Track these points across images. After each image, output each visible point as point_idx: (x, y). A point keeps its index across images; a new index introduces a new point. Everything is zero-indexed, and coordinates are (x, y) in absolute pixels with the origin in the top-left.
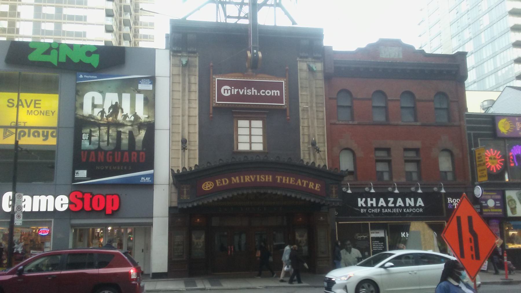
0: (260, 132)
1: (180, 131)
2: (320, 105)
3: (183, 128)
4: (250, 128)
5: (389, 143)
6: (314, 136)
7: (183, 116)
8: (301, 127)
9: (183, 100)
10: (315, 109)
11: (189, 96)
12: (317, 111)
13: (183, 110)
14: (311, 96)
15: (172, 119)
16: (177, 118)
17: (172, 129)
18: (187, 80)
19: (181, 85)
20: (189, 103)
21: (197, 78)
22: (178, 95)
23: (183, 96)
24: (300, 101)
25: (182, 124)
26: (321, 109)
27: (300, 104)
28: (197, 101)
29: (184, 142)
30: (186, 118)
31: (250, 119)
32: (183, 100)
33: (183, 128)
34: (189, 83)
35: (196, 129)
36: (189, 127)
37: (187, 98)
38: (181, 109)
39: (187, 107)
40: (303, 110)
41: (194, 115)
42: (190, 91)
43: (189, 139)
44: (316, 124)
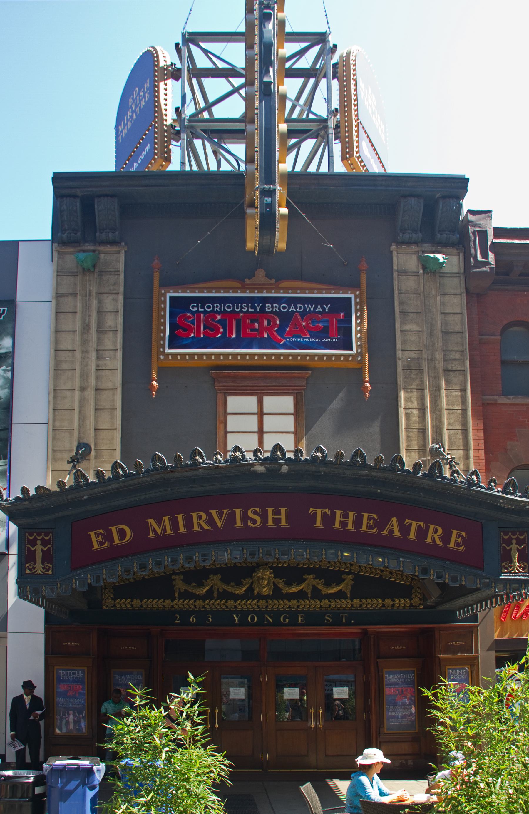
2: (457, 356)
4: (261, 414)
7: (83, 389)
9: (85, 352)
10: (440, 365)
11: (99, 341)
12: (446, 370)
13: (84, 376)
14: (431, 334)
15: (55, 397)
16: (68, 393)
17: (54, 421)
18: (94, 303)
19: (78, 315)
20: (98, 358)
21: (121, 298)
23: (84, 342)
24: (399, 346)
25: (81, 407)
26: (456, 366)
27: (399, 353)
28: (119, 354)
30: (90, 394)
31: (260, 392)
32: (85, 352)
36: (96, 418)
37: (93, 346)
39: (93, 367)
40: (407, 368)
41: (110, 385)
42: (100, 331)
43: (96, 444)
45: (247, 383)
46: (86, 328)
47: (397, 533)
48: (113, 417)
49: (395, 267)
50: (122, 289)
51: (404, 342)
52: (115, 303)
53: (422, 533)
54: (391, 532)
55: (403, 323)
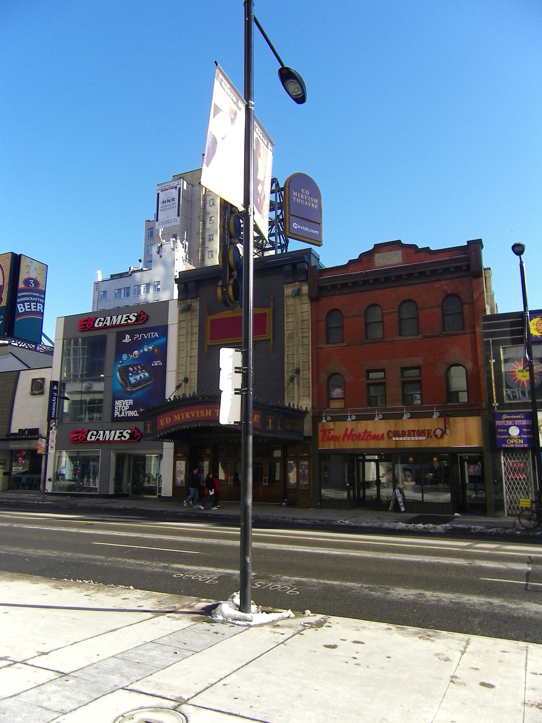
1: (184, 371)
3: (186, 368)
7: (187, 357)
8: (286, 356)
13: (187, 352)
20: (191, 344)
22: (183, 339)
23: (187, 339)
24: (285, 329)
26: (306, 335)
28: (197, 342)
29: (186, 380)
30: (189, 358)
33: (186, 368)
34: (192, 327)
35: (195, 368)
38: (184, 351)
40: (288, 338)
44: (300, 351)
46: (187, 333)
48: (195, 367)
50: (198, 317)
51: (287, 327)
52: (196, 323)
55: (287, 319)
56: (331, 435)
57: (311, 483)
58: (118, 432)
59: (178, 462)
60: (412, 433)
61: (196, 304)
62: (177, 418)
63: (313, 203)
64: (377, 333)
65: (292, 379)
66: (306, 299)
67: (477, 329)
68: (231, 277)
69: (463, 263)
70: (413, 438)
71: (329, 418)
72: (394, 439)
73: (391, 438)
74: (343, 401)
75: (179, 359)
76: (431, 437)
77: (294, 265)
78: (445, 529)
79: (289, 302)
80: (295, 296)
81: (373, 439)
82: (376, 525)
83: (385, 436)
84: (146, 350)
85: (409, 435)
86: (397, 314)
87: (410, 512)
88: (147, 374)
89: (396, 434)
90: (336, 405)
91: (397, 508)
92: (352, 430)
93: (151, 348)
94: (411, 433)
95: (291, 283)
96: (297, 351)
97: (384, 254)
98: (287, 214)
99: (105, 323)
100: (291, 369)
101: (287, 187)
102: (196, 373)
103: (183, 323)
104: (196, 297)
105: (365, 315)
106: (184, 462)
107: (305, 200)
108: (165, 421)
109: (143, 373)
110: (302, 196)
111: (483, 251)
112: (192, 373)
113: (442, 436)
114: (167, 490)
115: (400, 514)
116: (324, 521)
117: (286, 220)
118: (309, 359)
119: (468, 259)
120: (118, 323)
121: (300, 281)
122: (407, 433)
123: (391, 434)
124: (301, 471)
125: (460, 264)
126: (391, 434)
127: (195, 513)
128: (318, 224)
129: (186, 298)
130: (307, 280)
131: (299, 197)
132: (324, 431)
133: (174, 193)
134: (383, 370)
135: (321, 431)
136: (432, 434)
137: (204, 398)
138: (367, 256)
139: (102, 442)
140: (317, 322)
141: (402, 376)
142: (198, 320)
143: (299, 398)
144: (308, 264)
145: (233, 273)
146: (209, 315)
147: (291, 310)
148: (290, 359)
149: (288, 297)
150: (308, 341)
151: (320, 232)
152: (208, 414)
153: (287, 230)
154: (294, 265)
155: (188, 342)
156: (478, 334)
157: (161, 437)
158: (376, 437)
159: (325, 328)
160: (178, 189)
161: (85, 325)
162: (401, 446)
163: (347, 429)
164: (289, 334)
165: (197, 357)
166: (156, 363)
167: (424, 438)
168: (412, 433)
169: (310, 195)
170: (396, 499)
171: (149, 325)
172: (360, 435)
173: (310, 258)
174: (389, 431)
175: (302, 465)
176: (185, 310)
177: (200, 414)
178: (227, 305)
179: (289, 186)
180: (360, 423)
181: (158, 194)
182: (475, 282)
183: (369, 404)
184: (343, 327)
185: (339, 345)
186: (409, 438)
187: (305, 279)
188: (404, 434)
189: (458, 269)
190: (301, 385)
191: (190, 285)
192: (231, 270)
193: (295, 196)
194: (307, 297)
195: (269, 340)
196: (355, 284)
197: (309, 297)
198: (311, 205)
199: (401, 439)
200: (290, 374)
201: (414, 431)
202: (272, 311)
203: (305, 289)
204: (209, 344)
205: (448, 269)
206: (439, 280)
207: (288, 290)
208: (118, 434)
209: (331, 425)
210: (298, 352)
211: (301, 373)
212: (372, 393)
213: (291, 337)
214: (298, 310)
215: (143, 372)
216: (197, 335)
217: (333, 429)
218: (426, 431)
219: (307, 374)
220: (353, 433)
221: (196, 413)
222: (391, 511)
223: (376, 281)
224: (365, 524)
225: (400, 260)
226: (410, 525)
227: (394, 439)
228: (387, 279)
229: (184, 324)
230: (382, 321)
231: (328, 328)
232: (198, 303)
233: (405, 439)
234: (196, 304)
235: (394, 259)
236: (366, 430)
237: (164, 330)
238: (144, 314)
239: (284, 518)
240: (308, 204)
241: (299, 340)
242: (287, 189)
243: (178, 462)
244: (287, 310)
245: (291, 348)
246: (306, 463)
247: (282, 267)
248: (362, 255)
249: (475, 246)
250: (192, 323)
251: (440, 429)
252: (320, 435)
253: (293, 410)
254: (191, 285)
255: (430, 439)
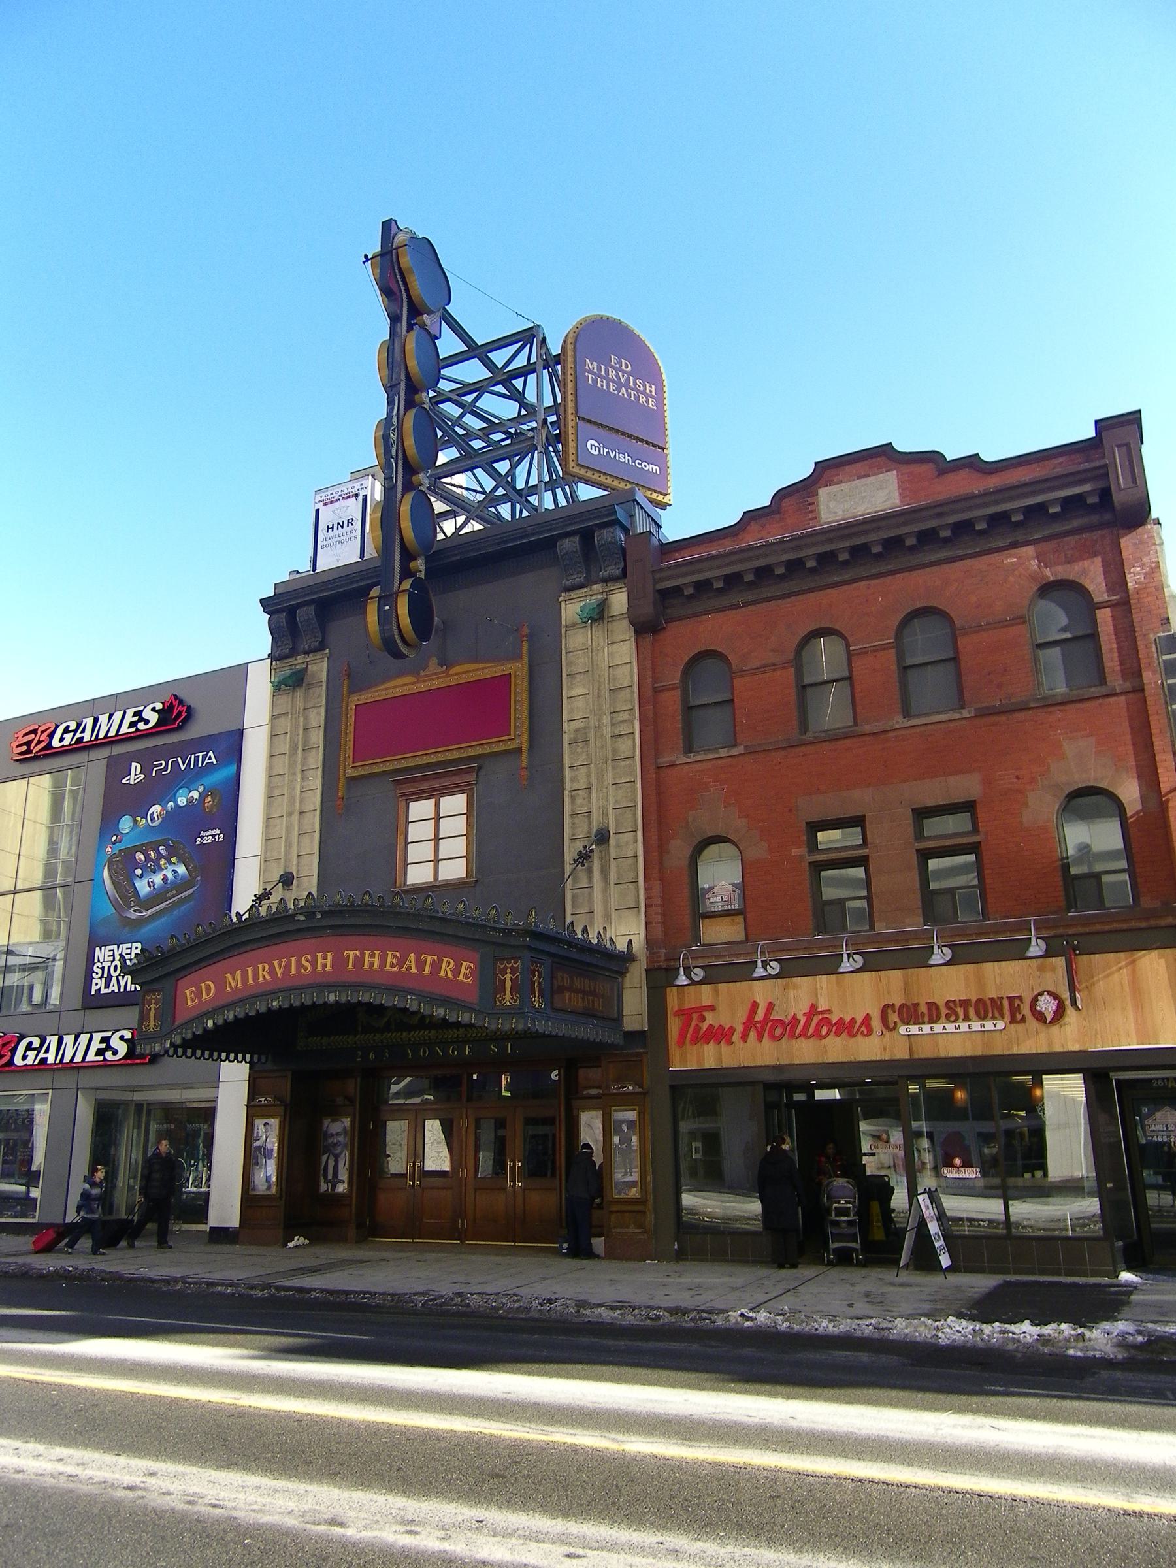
0: (460, 825)
2: (625, 716)
3: (289, 846)
5: (859, 799)
6: (605, 814)
7: (290, 814)
8: (566, 793)
16: (278, 820)
22: (281, 765)
23: (292, 764)
24: (565, 718)
28: (320, 771)
29: (287, 880)
30: (296, 817)
31: (436, 794)
33: (289, 846)
44: (609, 777)
45: (425, 786)
46: (294, 748)
47: (414, 970)
49: (563, 623)
51: (571, 711)
52: (317, 718)
53: (436, 967)
54: (409, 968)
55: (570, 688)
56: (705, 1026)
57: (650, 1178)
58: (97, 1037)
59: (259, 1123)
60: (960, 1011)
61: (319, 668)
62: (234, 981)
63: (644, 392)
64: (831, 711)
65: (584, 857)
66: (623, 630)
67: (1147, 676)
68: (406, 573)
69: (1087, 487)
70: (964, 1027)
71: (698, 974)
72: (902, 1030)
73: (895, 1028)
74: (741, 919)
75: (268, 820)
76: (1023, 1020)
77: (587, 536)
78: (1122, 1342)
79: (576, 640)
80: (593, 620)
81: (838, 1034)
82: (866, 1328)
83: (876, 1023)
84: (182, 801)
85: (952, 1016)
86: (893, 651)
87: (968, 1270)
88: (181, 869)
89: (910, 1014)
90: (717, 933)
91: (925, 1260)
92: (770, 1007)
93: (195, 794)
94: (957, 1009)
95: (581, 586)
96: (601, 777)
97: (845, 487)
98: (570, 417)
99: (78, 735)
100: (582, 832)
101: (570, 353)
102: (316, 859)
103: (282, 720)
104: (320, 648)
105: (797, 662)
106: (274, 1122)
107: (619, 385)
108: (199, 994)
109: (171, 868)
110: (612, 374)
111: (1148, 452)
112: (305, 860)
113: (1059, 1013)
114: (225, 1210)
115: (938, 1279)
116: (685, 1312)
117: (567, 439)
118: (634, 799)
119: (1103, 473)
120: (112, 733)
121: (606, 581)
122: (944, 1011)
123: (893, 1017)
124: (616, 1139)
125: (1077, 490)
126: (893, 1017)
127: (268, 1286)
128: (654, 445)
129: (293, 653)
130: (624, 574)
131: (603, 375)
132: (686, 1014)
133: (353, 508)
134: (858, 821)
135: (677, 1013)
136: (1026, 1009)
137: (310, 916)
138: (796, 497)
139: (53, 1068)
140: (656, 691)
141: (919, 835)
142: (323, 710)
143: (607, 916)
144: (626, 530)
145: (413, 564)
146: (352, 691)
147: (581, 662)
148: (579, 801)
149: (571, 626)
150: (632, 746)
151: (664, 468)
152: (324, 966)
153: (571, 457)
154: (587, 536)
155: (295, 774)
156: (1149, 690)
157: (186, 1044)
158: (845, 1028)
159: (681, 710)
160: (360, 498)
161: (28, 744)
162: (925, 1051)
163: (754, 1006)
164: (577, 731)
165: (318, 813)
166: (207, 837)
167: (1001, 1025)
168: (960, 1011)
169: (635, 374)
170: (922, 1224)
171: (194, 731)
172: (795, 1020)
173: (632, 516)
174: (886, 1007)
175: (622, 1122)
176: (289, 683)
177: (299, 965)
178: (398, 655)
179: (575, 344)
180: (795, 987)
181: (317, 511)
182: (1127, 543)
183: (821, 925)
184: (732, 701)
185: (723, 752)
186: (950, 1027)
187: (618, 572)
188: (933, 1014)
189: (1072, 504)
190: (613, 878)
191: (302, 614)
192: (408, 556)
193: (592, 372)
194: (626, 622)
195: (520, 749)
196: (764, 573)
197: (632, 622)
198: (637, 398)
199: (926, 1029)
200: (579, 846)
201: (965, 1003)
202: (526, 667)
203: (619, 600)
204: (350, 772)
205: (1042, 507)
206: (1014, 545)
207: (572, 609)
208: (96, 1045)
209: (706, 994)
210: (602, 781)
211: (612, 842)
212: (829, 893)
213: (581, 739)
214: (600, 664)
215: (170, 863)
216: (321, 750)
217: (712, 1008)
218: (1006, 1003)
219: (630, 844)
220: (774, 1016)
221: (288, 965)
222: (907, 1266)
223: (827, 560)
224: (824, 1326)
225: (897, 501)
226: (987, 1329)
227: (902, 1030)
228: (860, 552)
229: (285, 724)
230: (849, 678)
231: (689, 709)
232: (325, 664)
233: (938, 1028)
234: (319, 668)
235: (879, 496)
236: (813, 1007)
237: (231, 745)
238: (181, 702)
239: (550, 1301)
240: (629, 394)
241: (604, 747)
242: (570, 359)
243: (259, 1123)
244: (569, 664)
245: (583, 770)
246: (632, 1115)
247: (549, 544)
248: (781, 495)
249: (1121, 432)
250: (306, 718)
251: (1050, 993)
252: (674, 1026)
253: (585, 947)
254: (305, 614)
255: (1020, 1027)
